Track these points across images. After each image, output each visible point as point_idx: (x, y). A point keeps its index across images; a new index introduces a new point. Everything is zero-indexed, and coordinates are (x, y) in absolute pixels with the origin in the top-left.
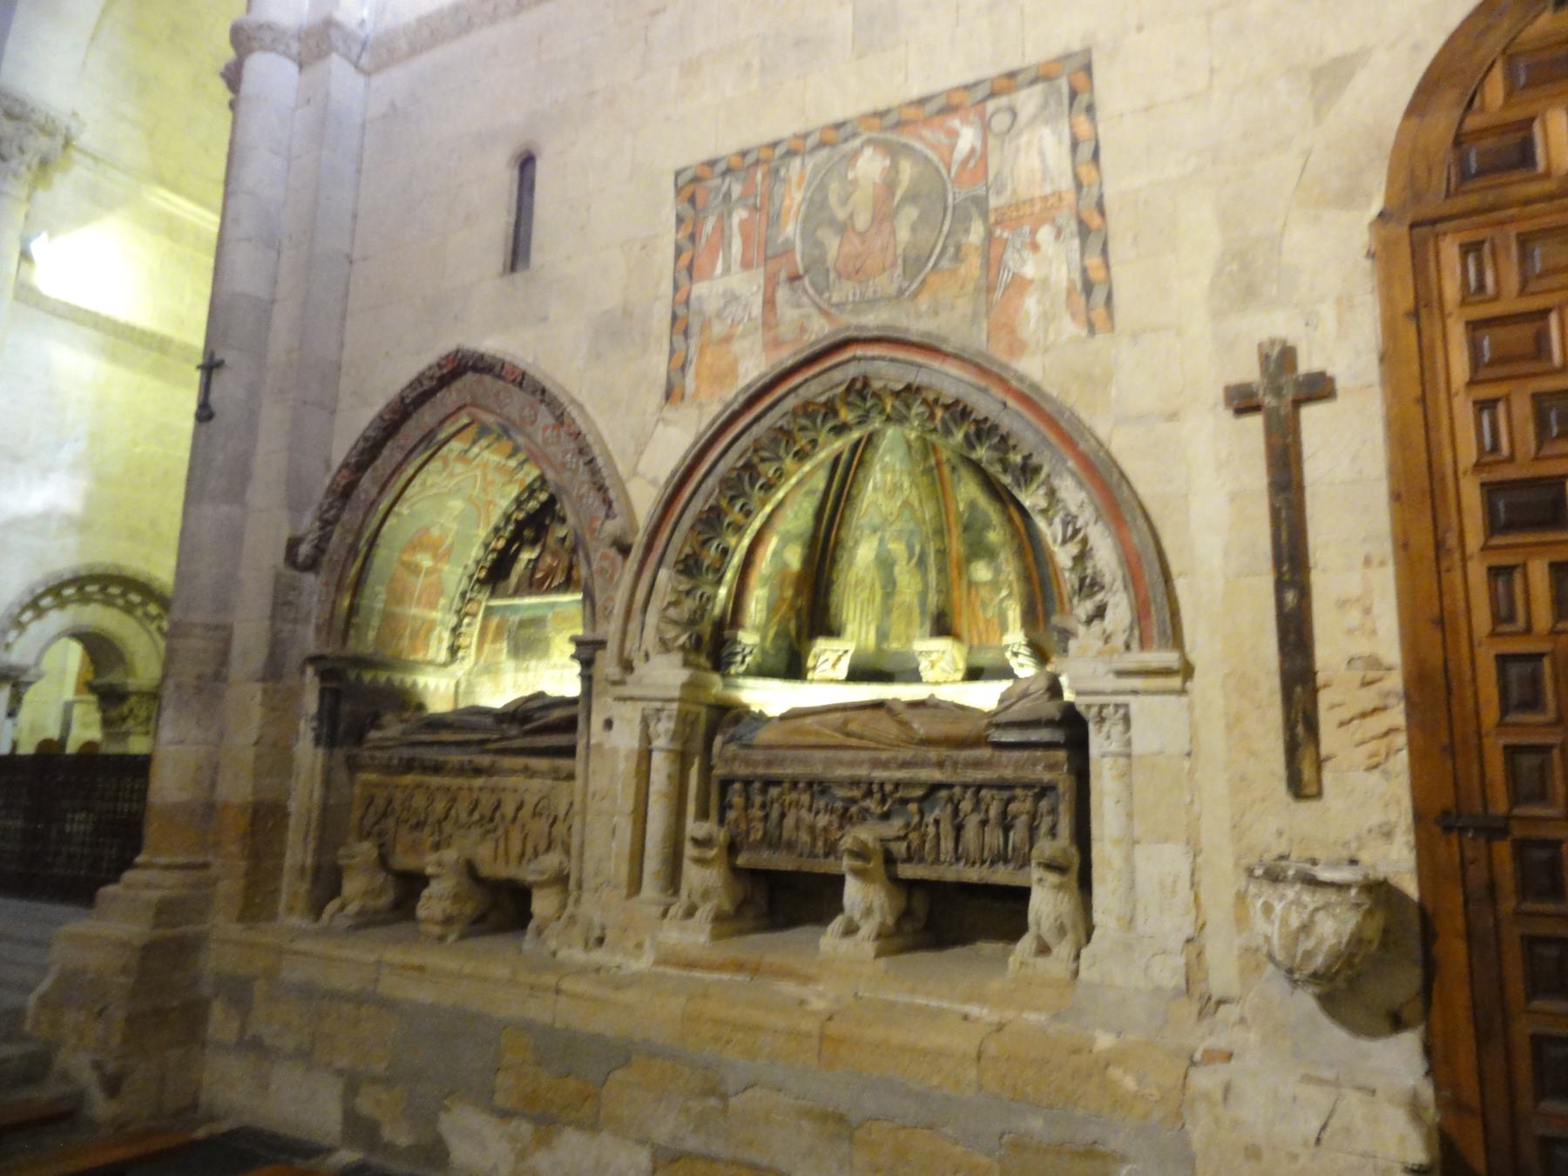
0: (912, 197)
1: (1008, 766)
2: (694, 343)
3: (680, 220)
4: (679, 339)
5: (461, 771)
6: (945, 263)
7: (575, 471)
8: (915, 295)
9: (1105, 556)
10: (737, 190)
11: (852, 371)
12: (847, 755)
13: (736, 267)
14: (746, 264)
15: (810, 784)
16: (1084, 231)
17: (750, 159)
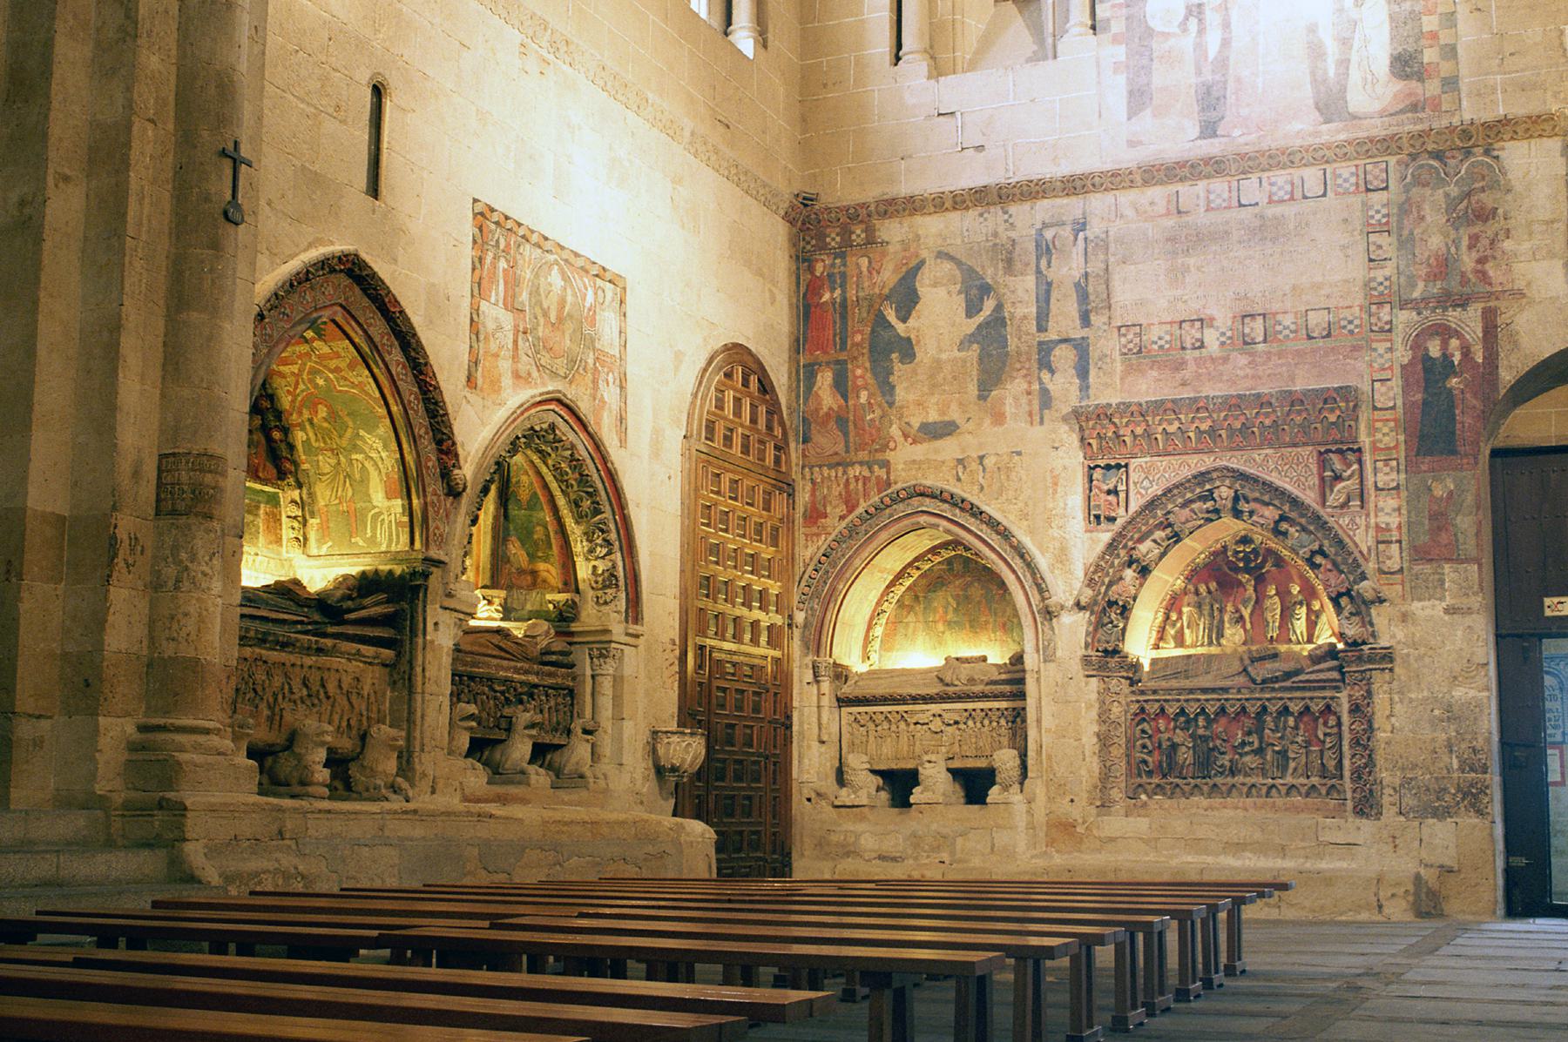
0: (570, 316)
1: (560, 677)
2: (481, 344)
3: (475, 242)
4: (474, 337)
5: (307, 650)
6: (581, 371)
7: (416, 412)
8: (571, 382)
9: (620, 573)
10: (502, 241)
11: (552, 418)
12: (505, 663)
13: (501, 304)
14: (506, 309)
15: (488, 679)
16: (622, 388)
17: (509, 224)
